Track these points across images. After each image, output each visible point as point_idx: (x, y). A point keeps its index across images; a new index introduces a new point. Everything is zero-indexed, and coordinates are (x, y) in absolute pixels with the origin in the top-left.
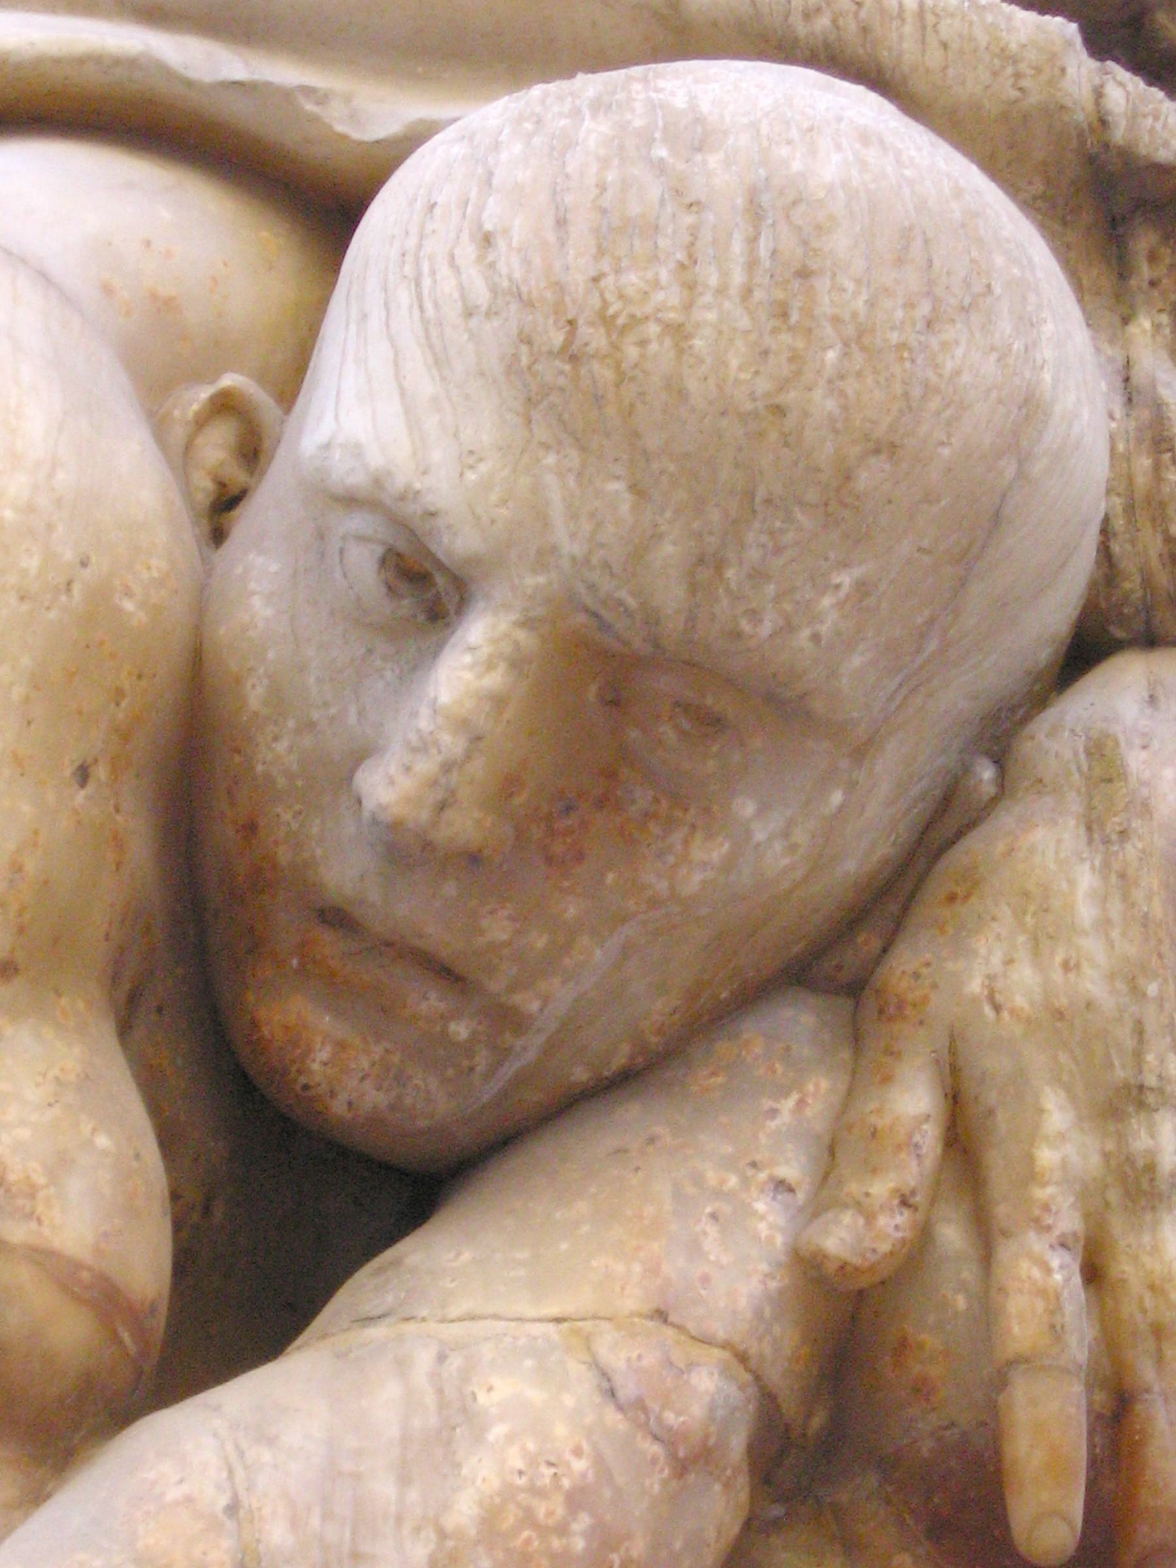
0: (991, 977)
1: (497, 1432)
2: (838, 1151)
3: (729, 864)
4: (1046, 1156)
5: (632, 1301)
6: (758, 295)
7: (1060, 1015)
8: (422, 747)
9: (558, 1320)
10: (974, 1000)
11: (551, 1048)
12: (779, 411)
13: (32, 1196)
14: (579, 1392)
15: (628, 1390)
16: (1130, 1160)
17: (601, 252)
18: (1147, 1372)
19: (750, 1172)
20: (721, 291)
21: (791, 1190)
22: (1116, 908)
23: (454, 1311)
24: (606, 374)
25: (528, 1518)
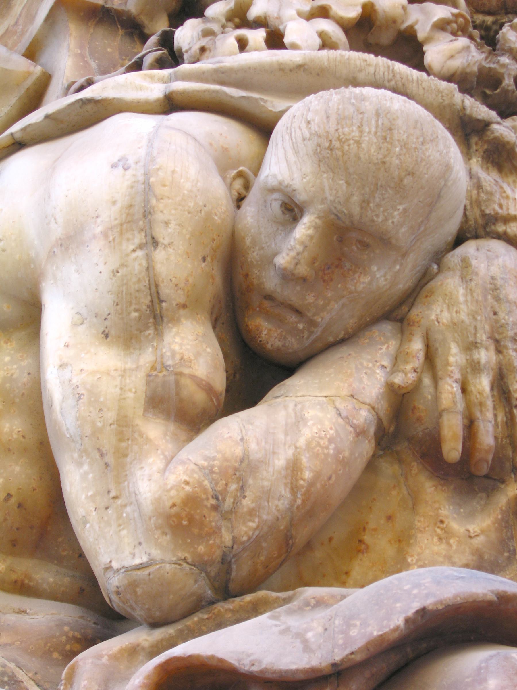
0: (437, 315)
1: (310, 423)
2: (398, 359)
3: (370, 283)
4: (451, 359)
5: (345, 392)
6: (379, 134)
7: (455, 324)
8: (291, 249)
9: (326, 397)
10: (433, 320)
11: (323, 332)
12: (384, 163)
13: (191, 362)
14: (331, 414)
15: (344, 414)
16: (473, 361)
17: (338, 123)
18: (478, 414)
19: (375, 363)
20: (369, 133)
21: (386, 368)
22: (469, 298)
23: (299, 394)
24: (339, 153)
25: (318, 444)
